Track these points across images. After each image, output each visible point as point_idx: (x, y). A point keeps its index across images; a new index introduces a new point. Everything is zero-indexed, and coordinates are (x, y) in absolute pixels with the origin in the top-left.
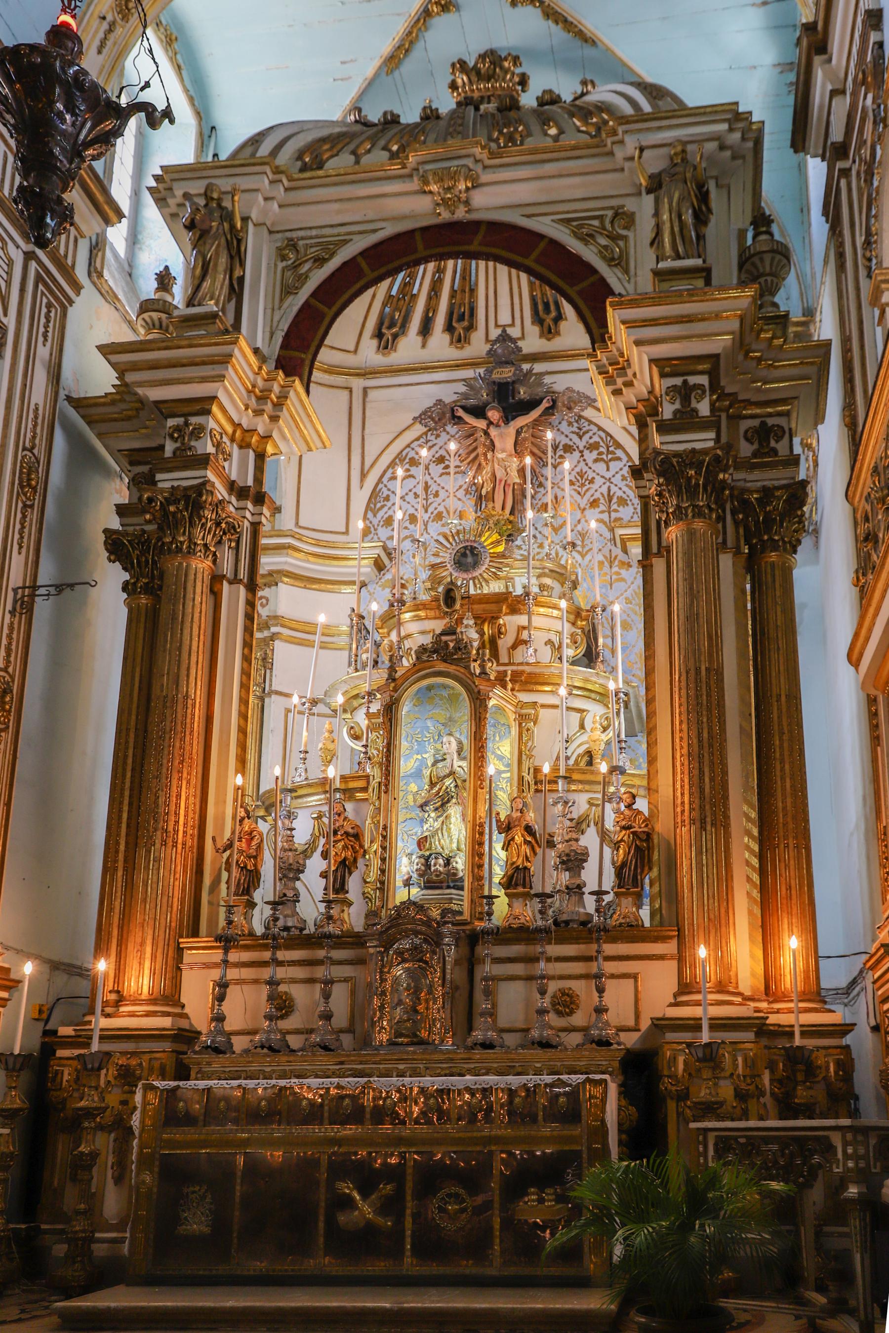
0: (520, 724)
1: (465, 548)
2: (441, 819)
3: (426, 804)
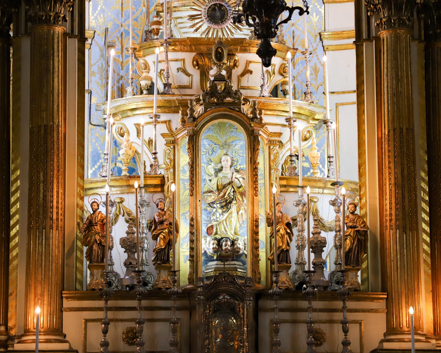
0: (269, 147)
2: (226, 215)
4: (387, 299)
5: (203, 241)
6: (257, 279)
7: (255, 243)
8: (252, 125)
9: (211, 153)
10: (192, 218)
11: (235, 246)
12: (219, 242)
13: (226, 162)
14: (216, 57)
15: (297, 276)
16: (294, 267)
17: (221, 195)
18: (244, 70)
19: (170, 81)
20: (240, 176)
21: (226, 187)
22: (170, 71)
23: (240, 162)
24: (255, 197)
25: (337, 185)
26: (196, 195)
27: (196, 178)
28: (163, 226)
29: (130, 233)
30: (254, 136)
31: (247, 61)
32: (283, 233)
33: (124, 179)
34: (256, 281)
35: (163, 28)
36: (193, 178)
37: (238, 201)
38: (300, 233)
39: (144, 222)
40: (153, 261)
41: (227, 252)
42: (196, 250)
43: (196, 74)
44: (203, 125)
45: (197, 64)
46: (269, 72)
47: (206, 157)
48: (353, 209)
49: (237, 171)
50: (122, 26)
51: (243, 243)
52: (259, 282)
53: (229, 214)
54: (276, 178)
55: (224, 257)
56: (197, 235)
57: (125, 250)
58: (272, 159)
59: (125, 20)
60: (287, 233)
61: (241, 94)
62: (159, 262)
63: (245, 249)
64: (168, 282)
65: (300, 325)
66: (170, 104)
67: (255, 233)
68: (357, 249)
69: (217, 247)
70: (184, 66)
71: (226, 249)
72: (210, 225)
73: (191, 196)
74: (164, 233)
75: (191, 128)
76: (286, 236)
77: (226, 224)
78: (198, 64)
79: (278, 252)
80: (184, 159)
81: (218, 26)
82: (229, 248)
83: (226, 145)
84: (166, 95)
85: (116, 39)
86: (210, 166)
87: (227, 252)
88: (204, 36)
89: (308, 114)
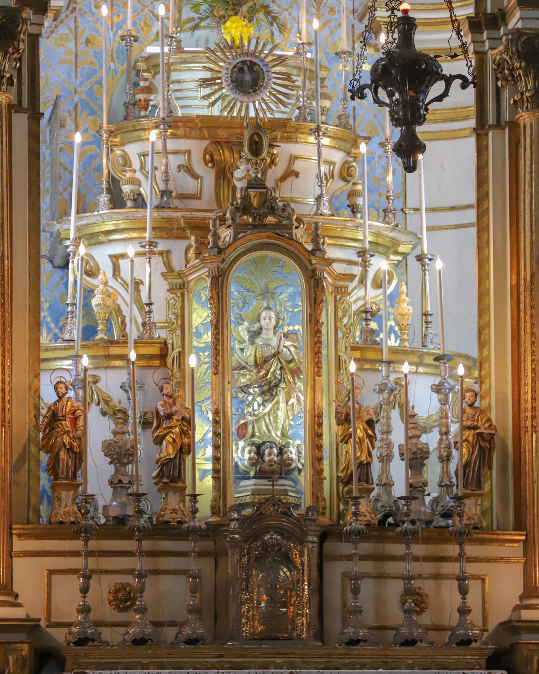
1: (244, 62)
2: (269, 406)
3: (248, 386)
4: (525, 542)
6: (321, 508)
7: (317, 451)
9: (241, 305)
10: (217, 409)
11: (285, 456)
13: (268, 320)
14: (251, 150)
15: (379, 504)
17: (262, 374)
18: (286, 171)
19: (171, 187)
21: (269, 360)
22: (169, 171)
23: (288, 321)
24: (317, 378)
25: (443, 359)
26: (223, 373)
27: (223, 345)
28: (169, 422)
29: (119, 433)
30: (315, 279)
31: (291, 155)
32: (361, 435)
33: (101, 345)
35: (157, 99)
36: (218, 345)
38: (385, 437)
40: (154, 478)
41: (271, 465)
42: (224, 461)
43: (208, 176)
45: (210, 159)
48: (472, 399)
49: (286, 336)
50: (76, 92)
51: (297, 450)
53: (275, 404)
54: (346, 348)
55: (265, 472)
56: (224, 437)
57: (110, 460)
59: (82, 83)
62: (165, 480)
64: (180, 513)
65: (390, 582)
67: (316, 435)
68: (477, 463)
69: (256, 457)
70: (189, 162)
71: (270, 461)
72: (242, 422)
73: (216, 374)
74: (173, 433)
75: (215, 264)
76: (367, 441)
78: (212, 160)
80: (200, 315)
81: (249, 98)
82: (275, 459)
83: (267, 292)
84: (165, 210)
85: (67, 114)
86: (240, 328)
87: (271, 465)
88: (225, 114)
89: (388, 244)
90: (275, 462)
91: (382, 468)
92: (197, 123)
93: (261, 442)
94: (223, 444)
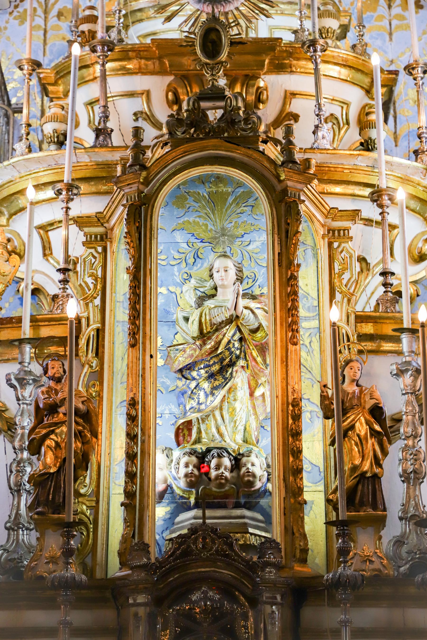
2: (221, 394)
3: (190, 367)
5: (160, 459)
6: (298, 551)
7: (291, 459)
8: (283, 177)
10: (133, 399)
11: (243, 470)
12: (202, 458)
15: (405, 549)
16: (394, 528)
17: (208, 346)
20: (259, 306)
21: (222, 328)
26: (144, 343)
31: (286, 91)
34: (295, 556)
36: (139, 303)
37: (252, 363)
38: (410, 443)
39: (26, 424)
41: (221, 486)
42: (142, 478)
44: (163, 181)
46: (337, 119)
47: (179, 271)
52: (304, 561)
56: (143, 442)
58: (337, 271)
60: (374, 433)
61: (259, 118)
63: (268, 480)
66: (109, 172)
69: (196, 472)
71: (219, 477)
76: (371, 442)
77: (222, 417)
79: (350, 482)
82: (227, 474)
83: (223, 235)
90: (226, 478)
91: (408, 492)
92: (155, 51)
93: (204, 449)
94: (142, 451)
